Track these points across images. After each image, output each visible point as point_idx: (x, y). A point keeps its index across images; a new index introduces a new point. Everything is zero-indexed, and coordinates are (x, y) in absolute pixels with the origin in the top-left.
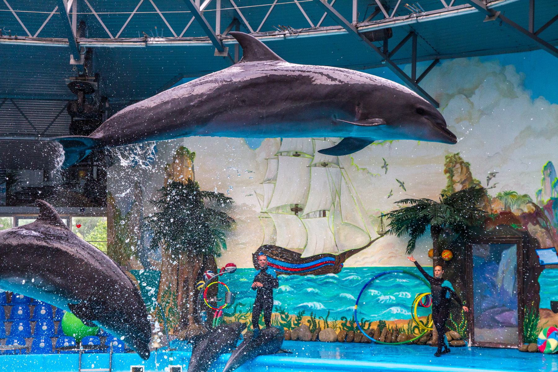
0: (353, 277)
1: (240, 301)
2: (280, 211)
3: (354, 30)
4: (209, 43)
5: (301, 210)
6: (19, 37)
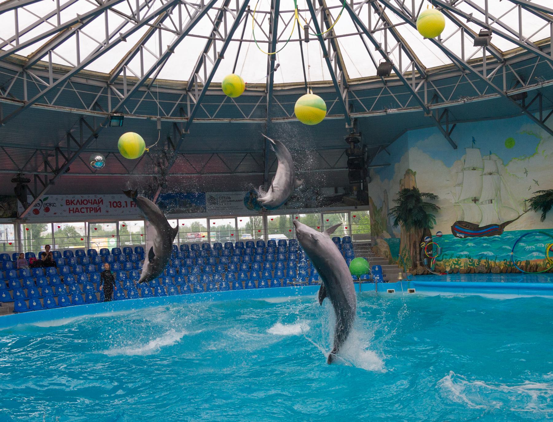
0: (510, 236)
1: (446, 253)
2: (466, 202)
3: (505, 94)
4: (421, 109)
5: (478, 200)
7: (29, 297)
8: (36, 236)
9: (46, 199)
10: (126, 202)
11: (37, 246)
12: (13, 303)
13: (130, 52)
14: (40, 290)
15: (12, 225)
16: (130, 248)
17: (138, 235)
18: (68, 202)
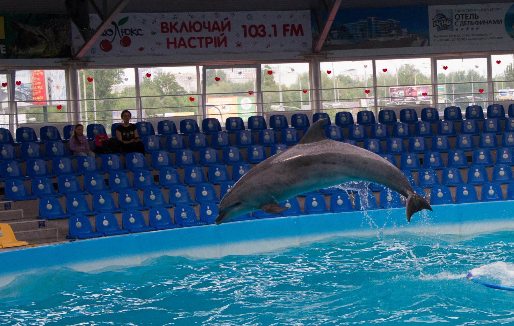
7: (97, 211)
8: (103, 93)
9: (124, 21)
10: (274, 26)
11: (106, 113)
12: (67, 221)
14: (115, 196)
15: (62, 72)
16: (281, 116)
18: (166, 28)
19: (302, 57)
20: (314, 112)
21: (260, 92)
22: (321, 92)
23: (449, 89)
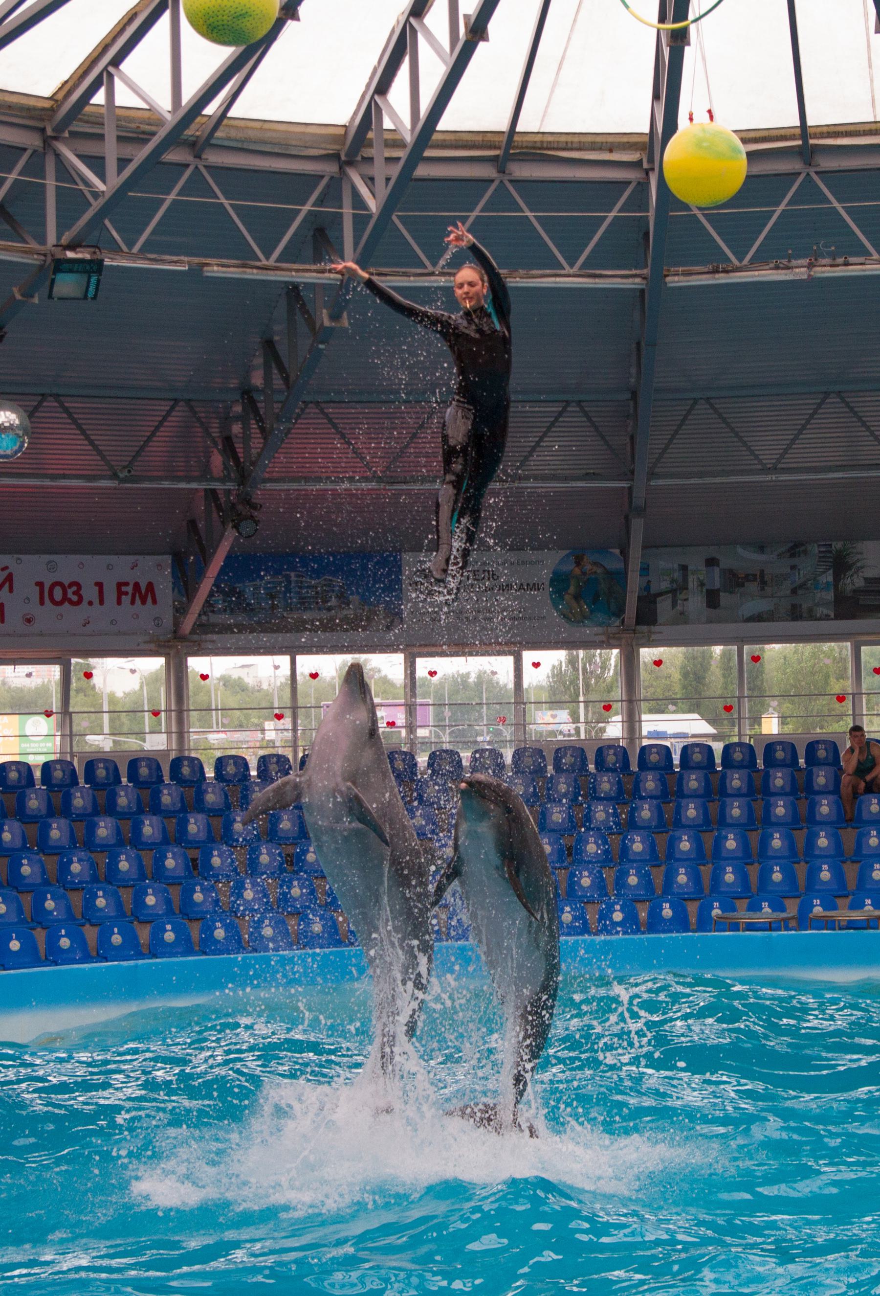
6: (851, 260)
10: (100, 585)
13: (131, 17)
17: (135, 712)
19: (152, 646)
20: (173, 755)
21: (66, 712)
22: (188, 716)
23: (439, 717)
